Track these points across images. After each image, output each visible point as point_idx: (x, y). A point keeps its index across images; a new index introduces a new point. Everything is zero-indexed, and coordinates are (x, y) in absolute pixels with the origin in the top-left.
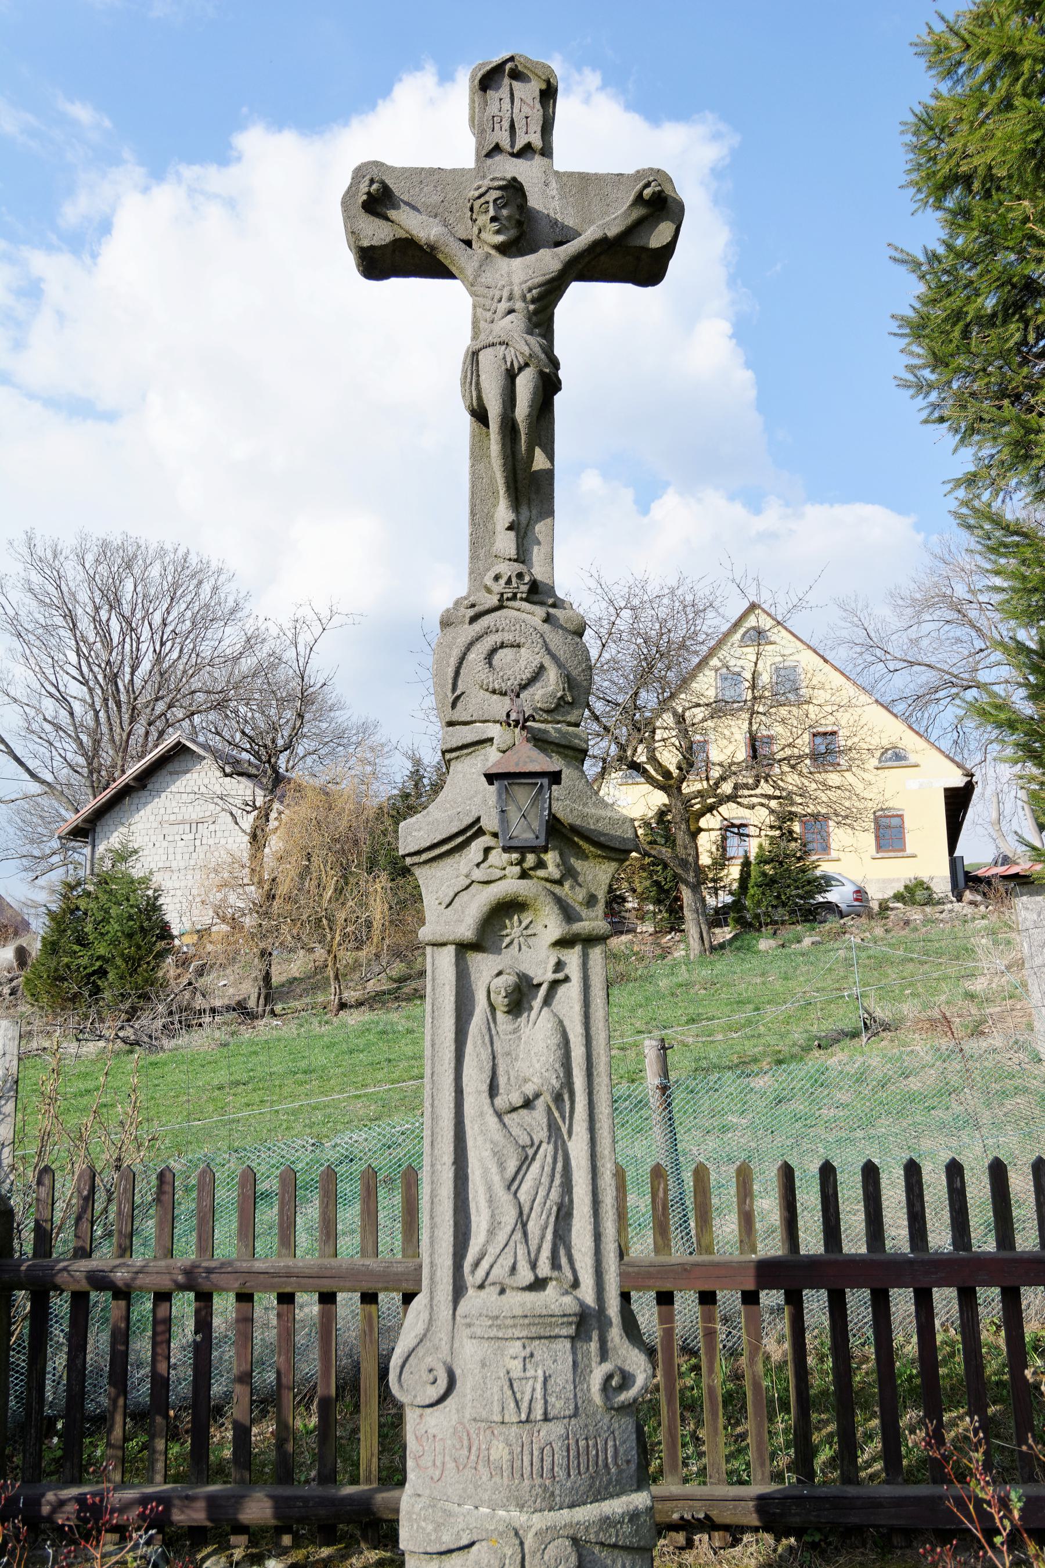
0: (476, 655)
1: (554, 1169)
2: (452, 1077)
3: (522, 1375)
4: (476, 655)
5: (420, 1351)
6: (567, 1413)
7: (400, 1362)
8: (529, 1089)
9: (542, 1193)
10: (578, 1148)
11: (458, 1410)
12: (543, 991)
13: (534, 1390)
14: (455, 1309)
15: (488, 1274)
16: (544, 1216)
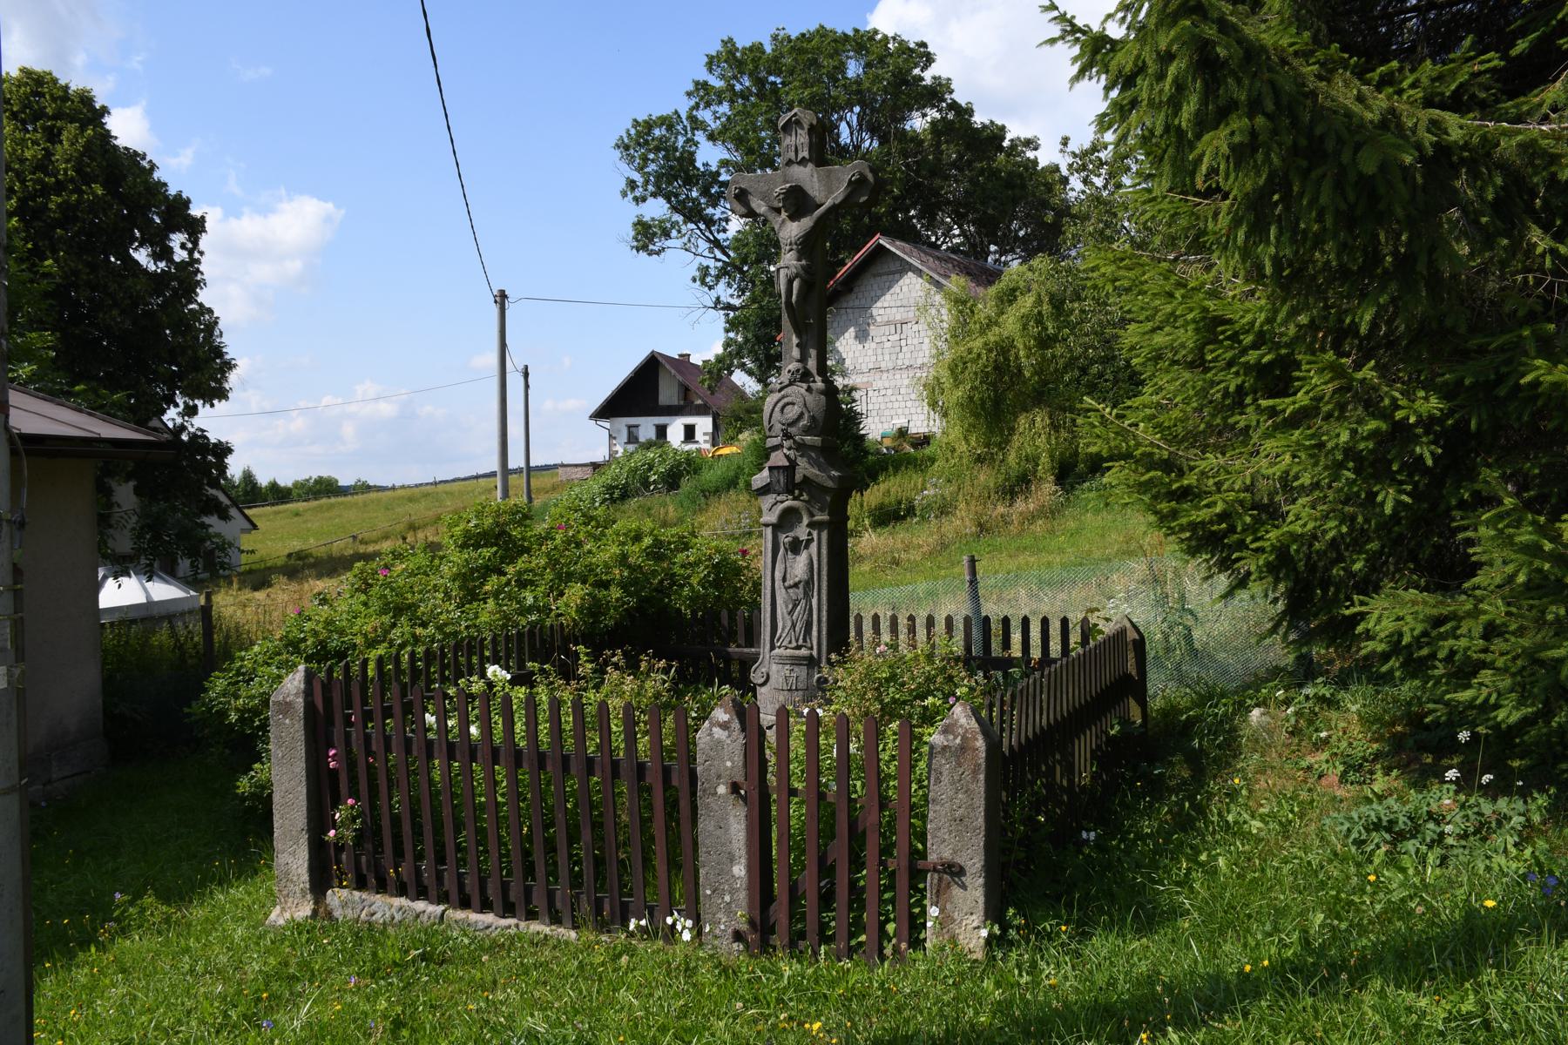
0: (777, 409)
4: (777, 409)
10: (814, 601)
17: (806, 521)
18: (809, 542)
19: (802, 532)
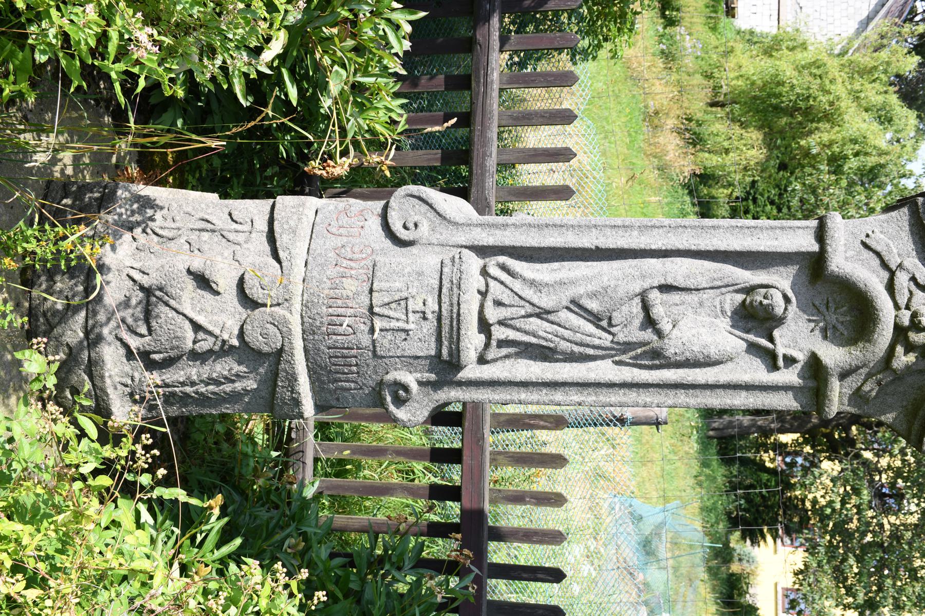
1: (588, 346)
2: (681, 247)
3: (410, 309)
5: (431, 215)
6: (378, 349)
7: (424, 196)
8: (665, 326)
9: (567, 334)
10: (604, 370)
11: (382, 250)
12: (764, 342)
13: (398, 320)
14: (466, 247)
15: (496, 279)
16: (544, 335)
17: (833, 356)
18: (771, 360)
19: (798, 337)
